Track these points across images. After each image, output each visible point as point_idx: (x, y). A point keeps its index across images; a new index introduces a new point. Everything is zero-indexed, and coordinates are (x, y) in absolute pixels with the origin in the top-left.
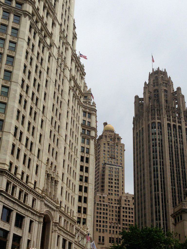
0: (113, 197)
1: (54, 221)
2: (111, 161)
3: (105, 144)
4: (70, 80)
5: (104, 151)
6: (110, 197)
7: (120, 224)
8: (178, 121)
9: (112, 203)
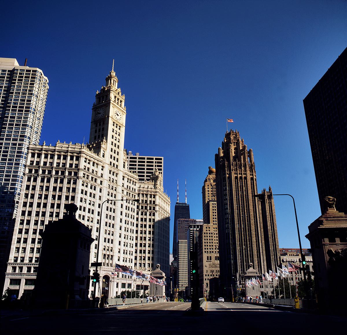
3: (208, 186)
4: (123, 191)
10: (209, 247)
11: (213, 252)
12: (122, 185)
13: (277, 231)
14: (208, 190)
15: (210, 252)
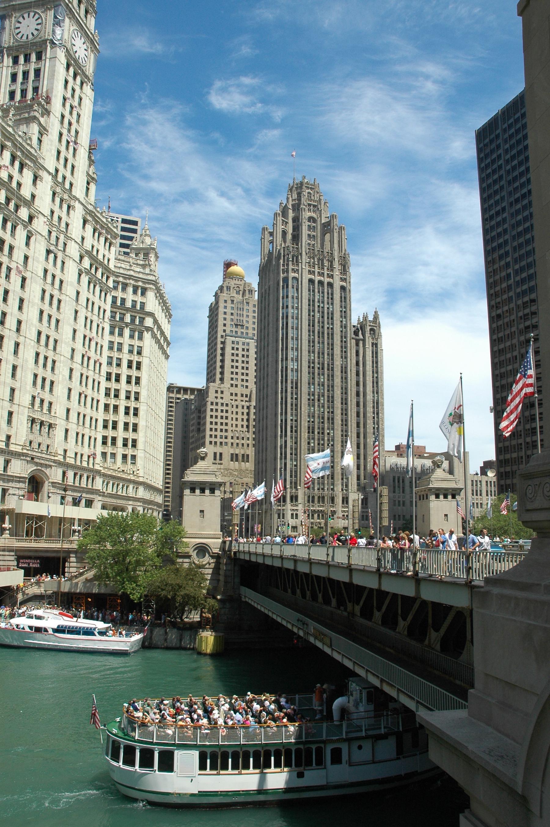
0: (239, 390)
1: (50, 480)
2: (237, 330)
3: (226, 301)
4: (81, 257)
5: (225, 313)
6: (234, 390)
7: (248, 432)
8: (328, 274)
9: (236, 400)
10: (219, 433)
11: (226, 444)
12: (79, 240)
13: (383, 405)
14: (225, 310)
15: (221, 443)
